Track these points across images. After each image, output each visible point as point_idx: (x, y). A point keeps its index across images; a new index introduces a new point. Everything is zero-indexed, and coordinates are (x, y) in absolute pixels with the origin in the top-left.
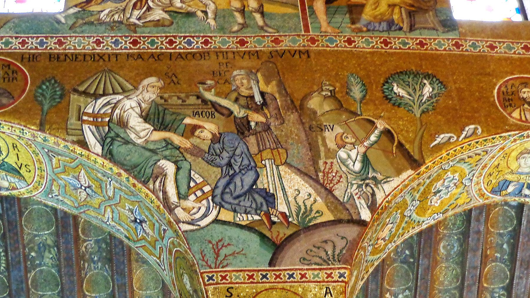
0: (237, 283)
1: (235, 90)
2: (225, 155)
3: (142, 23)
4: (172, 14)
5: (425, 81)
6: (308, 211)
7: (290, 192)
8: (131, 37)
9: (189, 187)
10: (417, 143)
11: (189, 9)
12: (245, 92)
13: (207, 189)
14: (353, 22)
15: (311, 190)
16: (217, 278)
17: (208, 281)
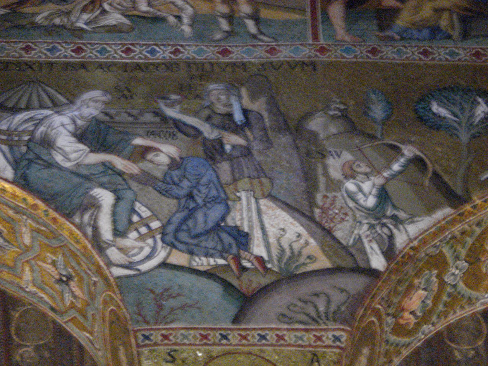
0: (184, 344)
1: (208, 107)
2: (185, 184)
3: (92, 28)
4: (135, 18)
5: (480, 100)
6: (294, 256)
7: (272, 231)
8: (74, 43)
9: (130, 222)
10: (460, 174)
11: (159, 13)
12: (221, 109)
13: (155, 224)
14: (382, 28)
15: (301, 229)
16: (157, 337)
17: (142, 341)
